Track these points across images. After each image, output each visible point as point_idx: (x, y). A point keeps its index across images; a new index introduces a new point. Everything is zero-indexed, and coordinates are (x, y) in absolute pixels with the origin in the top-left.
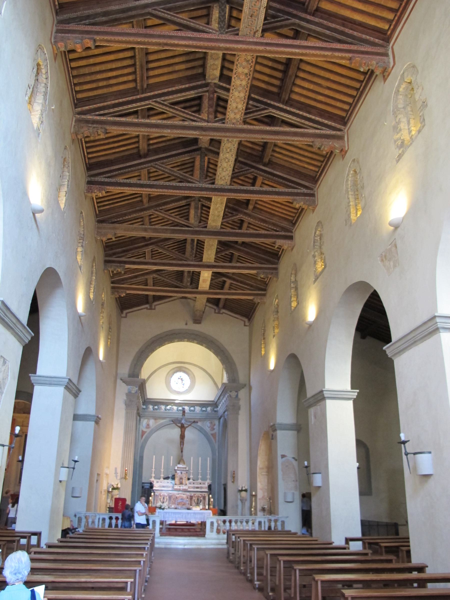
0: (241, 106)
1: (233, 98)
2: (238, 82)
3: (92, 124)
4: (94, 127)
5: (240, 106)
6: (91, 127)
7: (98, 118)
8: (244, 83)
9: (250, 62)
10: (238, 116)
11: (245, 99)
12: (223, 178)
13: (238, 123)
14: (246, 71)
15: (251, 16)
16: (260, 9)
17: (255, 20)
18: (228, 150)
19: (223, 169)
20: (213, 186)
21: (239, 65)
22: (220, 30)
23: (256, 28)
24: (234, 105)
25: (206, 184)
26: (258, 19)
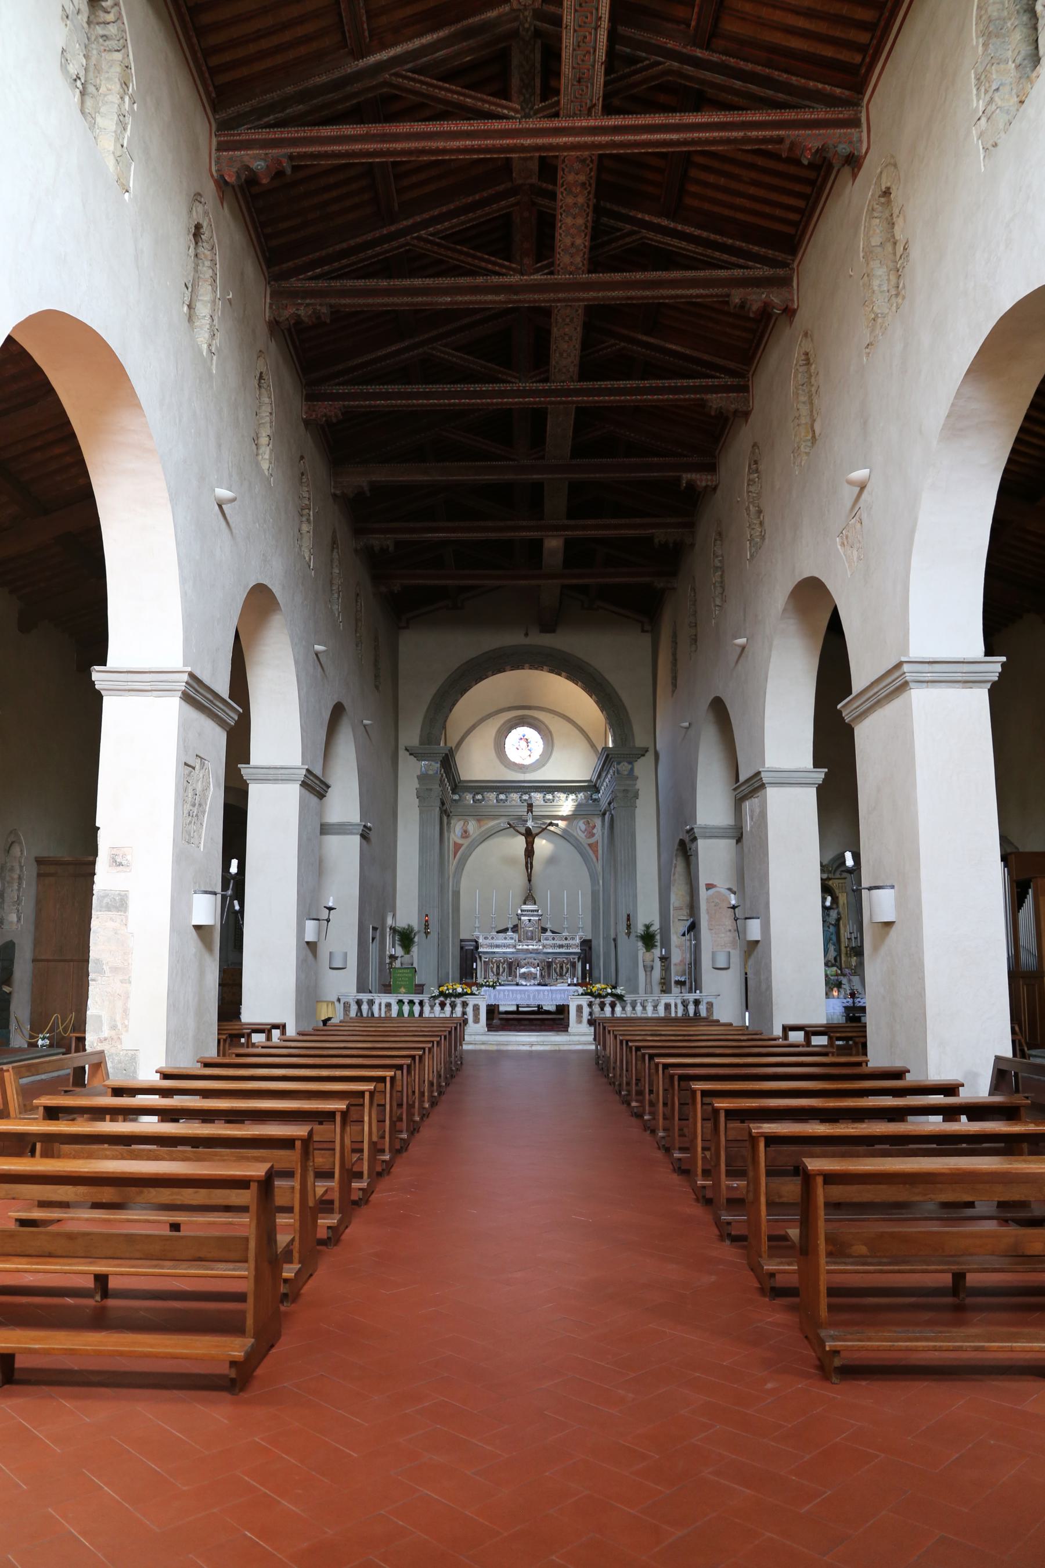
0: (581, 241)
1: (563, 228)
2: (570, 200)
3: (303, 298)
4: (308, 305)
5: (579, 241)
6: (302, 304)
7: (313, 284)
8: (581, 200)
9: (588, 162)
11: (586, 227)
12: (564, 370)
13: (580, 271)
14: (582, 178)
15: (579, 81)
16: (594, 66)
17: (587, 87)
18: (568, 320)
19: (561, 355)
20: (547, 386)
21: (567, 170)
22: (523, 109)
23: (591, 100)
24: (568, 241)
25: (533, 383)
26: (593, 85)
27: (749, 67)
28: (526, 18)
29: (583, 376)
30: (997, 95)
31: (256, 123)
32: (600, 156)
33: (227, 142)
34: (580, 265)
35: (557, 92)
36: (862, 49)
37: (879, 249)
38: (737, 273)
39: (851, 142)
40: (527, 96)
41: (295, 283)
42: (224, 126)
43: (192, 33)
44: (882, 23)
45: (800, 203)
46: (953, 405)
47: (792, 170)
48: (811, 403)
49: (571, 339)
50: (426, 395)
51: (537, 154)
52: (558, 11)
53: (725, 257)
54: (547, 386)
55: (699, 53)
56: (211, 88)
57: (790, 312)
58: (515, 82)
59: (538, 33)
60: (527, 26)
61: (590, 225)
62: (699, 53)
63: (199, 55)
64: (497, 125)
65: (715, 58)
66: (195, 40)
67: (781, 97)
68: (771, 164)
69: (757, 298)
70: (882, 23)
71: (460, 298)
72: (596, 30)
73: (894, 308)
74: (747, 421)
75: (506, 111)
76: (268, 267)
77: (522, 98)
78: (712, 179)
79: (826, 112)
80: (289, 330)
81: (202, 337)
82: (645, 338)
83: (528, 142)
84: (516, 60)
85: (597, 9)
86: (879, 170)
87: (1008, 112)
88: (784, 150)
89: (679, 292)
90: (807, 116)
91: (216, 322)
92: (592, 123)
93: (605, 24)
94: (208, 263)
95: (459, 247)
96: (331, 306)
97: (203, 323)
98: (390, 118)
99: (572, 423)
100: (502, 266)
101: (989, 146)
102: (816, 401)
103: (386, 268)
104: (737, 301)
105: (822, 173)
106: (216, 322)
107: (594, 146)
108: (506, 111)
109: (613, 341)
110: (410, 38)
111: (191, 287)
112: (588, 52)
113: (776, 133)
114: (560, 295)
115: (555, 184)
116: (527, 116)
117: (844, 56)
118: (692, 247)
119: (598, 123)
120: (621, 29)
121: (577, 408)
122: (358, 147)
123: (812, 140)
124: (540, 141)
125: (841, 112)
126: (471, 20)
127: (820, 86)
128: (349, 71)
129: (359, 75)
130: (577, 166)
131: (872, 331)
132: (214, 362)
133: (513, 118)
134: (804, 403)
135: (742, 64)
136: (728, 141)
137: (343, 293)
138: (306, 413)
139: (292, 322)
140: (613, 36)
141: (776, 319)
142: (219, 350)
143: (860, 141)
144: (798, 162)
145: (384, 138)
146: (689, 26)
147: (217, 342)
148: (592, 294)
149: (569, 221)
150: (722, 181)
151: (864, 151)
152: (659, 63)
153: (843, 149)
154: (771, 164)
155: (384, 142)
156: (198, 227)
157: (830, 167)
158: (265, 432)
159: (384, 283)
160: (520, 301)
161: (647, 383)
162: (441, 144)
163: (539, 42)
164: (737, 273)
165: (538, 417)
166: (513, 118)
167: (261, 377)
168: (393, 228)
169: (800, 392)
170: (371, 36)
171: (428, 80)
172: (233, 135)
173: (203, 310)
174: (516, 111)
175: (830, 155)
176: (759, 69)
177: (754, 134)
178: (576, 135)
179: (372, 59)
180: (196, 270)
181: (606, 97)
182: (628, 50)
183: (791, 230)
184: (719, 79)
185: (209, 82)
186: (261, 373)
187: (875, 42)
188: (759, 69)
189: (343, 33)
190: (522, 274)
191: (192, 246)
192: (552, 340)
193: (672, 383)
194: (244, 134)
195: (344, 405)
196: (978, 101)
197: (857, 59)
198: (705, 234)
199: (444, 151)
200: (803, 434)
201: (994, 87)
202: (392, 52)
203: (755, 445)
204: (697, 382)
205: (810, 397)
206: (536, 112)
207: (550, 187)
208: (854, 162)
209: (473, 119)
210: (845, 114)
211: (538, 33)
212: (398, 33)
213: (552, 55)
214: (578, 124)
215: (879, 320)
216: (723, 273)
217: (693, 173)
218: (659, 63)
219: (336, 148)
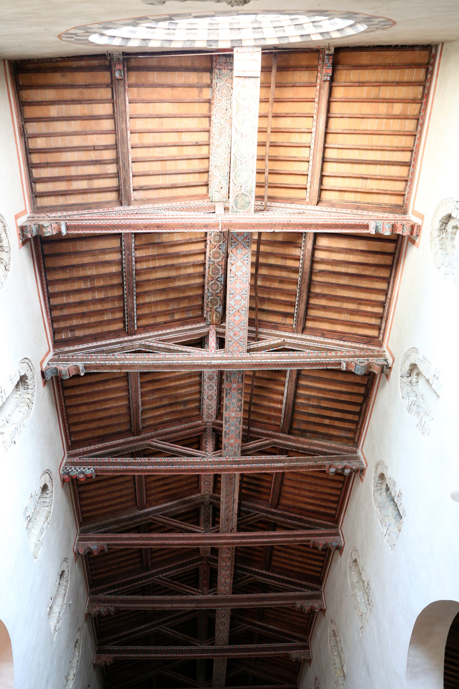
0: (229, 581)
1: (221, 575)
2: (224, 564)
3: (104, 603)
4: (105, 606)
5: (228, 581)
6: (102, 606)
7: (109, 597)
8: (228, 564)
10: (228, 588)
11: (231, 575)
12: (222, 639)
13: (229, 594)
14: (229, 555)
15: (227, 520)
16: (233, 515)
18: (223, 615)
19: (220, 632)
20: (213, 647)
22: (204, 529)
24: (223, 580)
25: (207, 646)
26: (232, 522)
27: (293, 515)
28: (207, 498)
29: (231, 642)
30: (389, 527)
31: (96, 531)
32: (236, 547)
33: (83, 538)
34: (229, 591)
35: (218, 523)
36: (335, 509)
37: (357, 584)
38: (298, 593)
39: (337, 542)
40: (207, 525)
41: (101, 596)
42: (82, 532)
43: (78, 500)
44: (340, 501)
45: (321, 564)
46: (408, 660)
47: (315, 551)
48: (340, 656)
49: (225, 624)
50: (156, 652)
51: (210, 546)
52: (219, 496)
53: (292, 586)
54: (213, 647)
55: (273, 510)
56: (81, 518)
57: (323, 611)
58: (202, 519)
59: (211, 503)
60: (207, 500)
61: (232, 574)
62: (273, 510)
63: (79, 507)
64: (194, 535)
65: (280, 512)
66: (78, 502)
67: (307, 525)
68: (306, 549)
69: (308, 605)
70: (340, 501)
71: (175, 605)
72: (233, 503)
73: (369, 611)
74: (310, 665)
75: (198, 530)
76: (90, 588)
77: (204, 525)
78: (283, 555)
79: (325, 531)
80: (95, 618)
81: (53, 622)
82: (259, 623)
83: (206, 542)
84: (202, 511)
85: (234, 497)
86: (350, 552)
87: (396, 533)
88: (311, 544)
89: (273, 602)
90: (318, 532)
91: (61, 615)
92: (232, 535)
93: (237, 501)
94: (63, 588)
95: (175, 582)
96: (116, 607)
97: (55, 616)
98: (150, 531)
99: (226, 666)
100: (194, 591)
101: (392, 545)
102: (342, 655)
103: (143, 591)
104: (299, 606)
105: (328, 552)
106: (61, 615)
107: (233, 544)
108: (198, 530)
109: (244, 625)
110: (162, 504)
111: (53, 599)
112: (231, 511)
113: (306, 538)
114: (220, 604)
115: (218, 556)
116: (206, 532)
117: (329, 511)
118: (277, 582)
119: (235, 535)
120: (243, 502)
121: (228, 659)
122: (136, 542)
123: (321, 541)
124: (211, 541)
125: (331, 530)
126: (185, 498)
127: (321, 521)
128: (137, 514)
129: (140, 516)
130: (226, 551)
131: (362, 621)
132: (56, 635)
133: (200, 533)
134: (336, 656)
135: (290, 514)
136: (288, 542)
137: (122, 601)
138: (96, 660)
139: (97, 614)
140: (240, 505)
141: (317, 614)
142: (59, 629)
143: (341, 541)
144: (317, 548)
145: (147, 539)
146: (269, 501)
147: (59, 625)
148: (234, 604)
149: (224, 572)
150: (287, 556)
151: (343, 545)
152: (258, 514)
153: (335, 544)
154: (306, 549)
155: (147, 540)
156: (63, 572)
157: (330, 551)
158: (73, 671)
159: (141, 598)
160: (202, 607)
161: (261, 645)
162: (171, 542)
163: (211, 506)
164: (298, 593)
165: (209, 663)
166: (200, 533)
167: (77, 642)
168: (147, 573)
169: (334, 650)
170: (147, 503)
171: (168, 518)
172: (86, 535)
173: (56, 609)
174: (202, 530)
175: (330, 546)
176: (297, 516)
177: (298, 539)
178: (226, 539)
179: (146, 510)
180: (58, 591)
181: (238, 525)
182: (246, 509)
183: (318, 575)
184: (282, 519)
185: (81, 516)
186: (77, 640)
187: (339, 507)
188: (297, 516)
189: (136, 501)
190: (203, 595)
191: (58, 581)
192: (216, 625)
193: (273, 645)
194: (90, 535)
195: (115, 657)
196: (383, 529)
197: (334, 512)
198: (282, 577)
199: (172, 545)
200: (339, 673)
201: (388, 525)
202: (154, 508)
203: (316, 678)
204: (285, 644)
205: (339, 652)
206: (210, 531)
207: (216, 558)
208: (340, 549)
209: (185, 533)
210: (333, 531)
211: (211, 503)
212: (157, 502)
213: (216, 510)
214: (227, 535)
215: (364, 616)
216: (291, 594)
217: (275, 552)
218: (258, 514)
219: (127, 542)
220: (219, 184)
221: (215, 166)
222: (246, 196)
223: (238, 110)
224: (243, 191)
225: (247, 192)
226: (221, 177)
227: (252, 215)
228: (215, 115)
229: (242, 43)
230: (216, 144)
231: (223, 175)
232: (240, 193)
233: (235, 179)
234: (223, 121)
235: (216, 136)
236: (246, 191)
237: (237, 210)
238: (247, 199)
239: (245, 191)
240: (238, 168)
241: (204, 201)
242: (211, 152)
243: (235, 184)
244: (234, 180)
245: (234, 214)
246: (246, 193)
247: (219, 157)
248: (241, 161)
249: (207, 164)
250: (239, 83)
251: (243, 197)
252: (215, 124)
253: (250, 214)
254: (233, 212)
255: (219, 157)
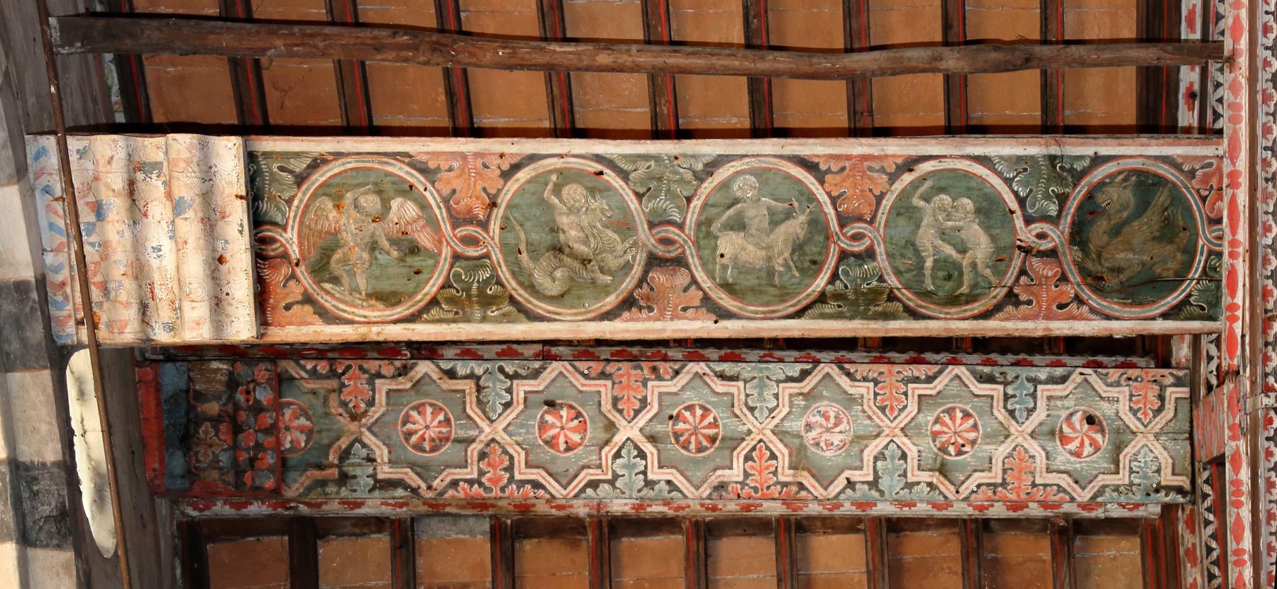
220: (1064, 440)
221: (936, 478)
222: (1090, 210)
223: (487, 302)
224: (1057, 236)
225: (1062, 199)
226: (1014, 427)
227: (1233, 154)
228: (594, 484)
229: (20, 287)
230: (786, 475)
231: (1001, 414)
232: (1070, 255)
233: (971, 298)
234: (628, 431)
235: (735, 474)
236: (1053, 209)
237: (1196, 272)
238: (1119, 197)
239: (1055, 221)
240: (893, 281)
241: (1191, 553)
242: (848, 509)
243: (1011, 298)
244: (977, 307)
245: (1226, 300)
246: (1072, 206)
247: (873, 448)
248: (844, 255)
249: (933, 535)
250: (308, 299)
251: (1098, 232)
252: (649, 484)
253: (1227, 167)
254: (1215, 302)
255: (873, 448)
